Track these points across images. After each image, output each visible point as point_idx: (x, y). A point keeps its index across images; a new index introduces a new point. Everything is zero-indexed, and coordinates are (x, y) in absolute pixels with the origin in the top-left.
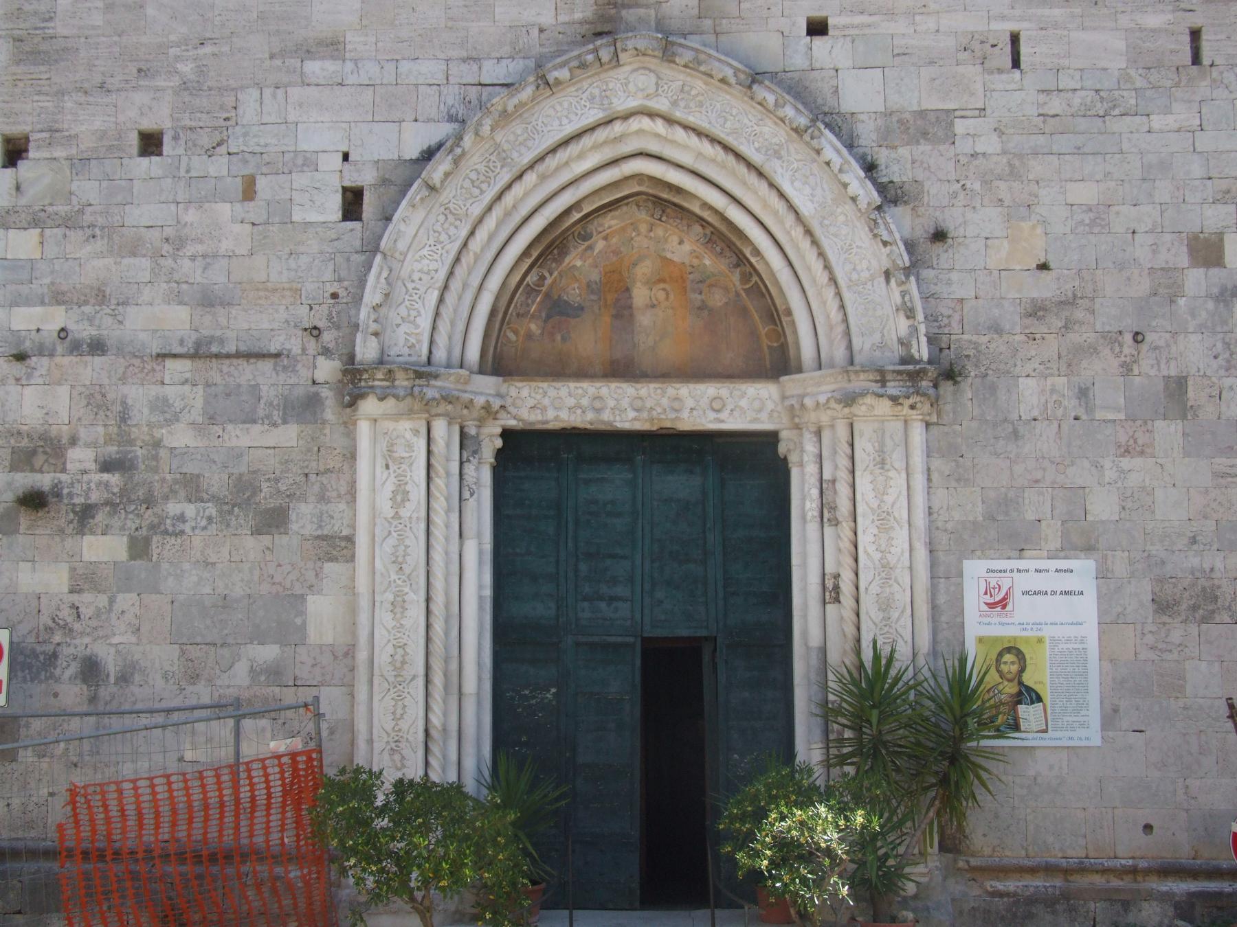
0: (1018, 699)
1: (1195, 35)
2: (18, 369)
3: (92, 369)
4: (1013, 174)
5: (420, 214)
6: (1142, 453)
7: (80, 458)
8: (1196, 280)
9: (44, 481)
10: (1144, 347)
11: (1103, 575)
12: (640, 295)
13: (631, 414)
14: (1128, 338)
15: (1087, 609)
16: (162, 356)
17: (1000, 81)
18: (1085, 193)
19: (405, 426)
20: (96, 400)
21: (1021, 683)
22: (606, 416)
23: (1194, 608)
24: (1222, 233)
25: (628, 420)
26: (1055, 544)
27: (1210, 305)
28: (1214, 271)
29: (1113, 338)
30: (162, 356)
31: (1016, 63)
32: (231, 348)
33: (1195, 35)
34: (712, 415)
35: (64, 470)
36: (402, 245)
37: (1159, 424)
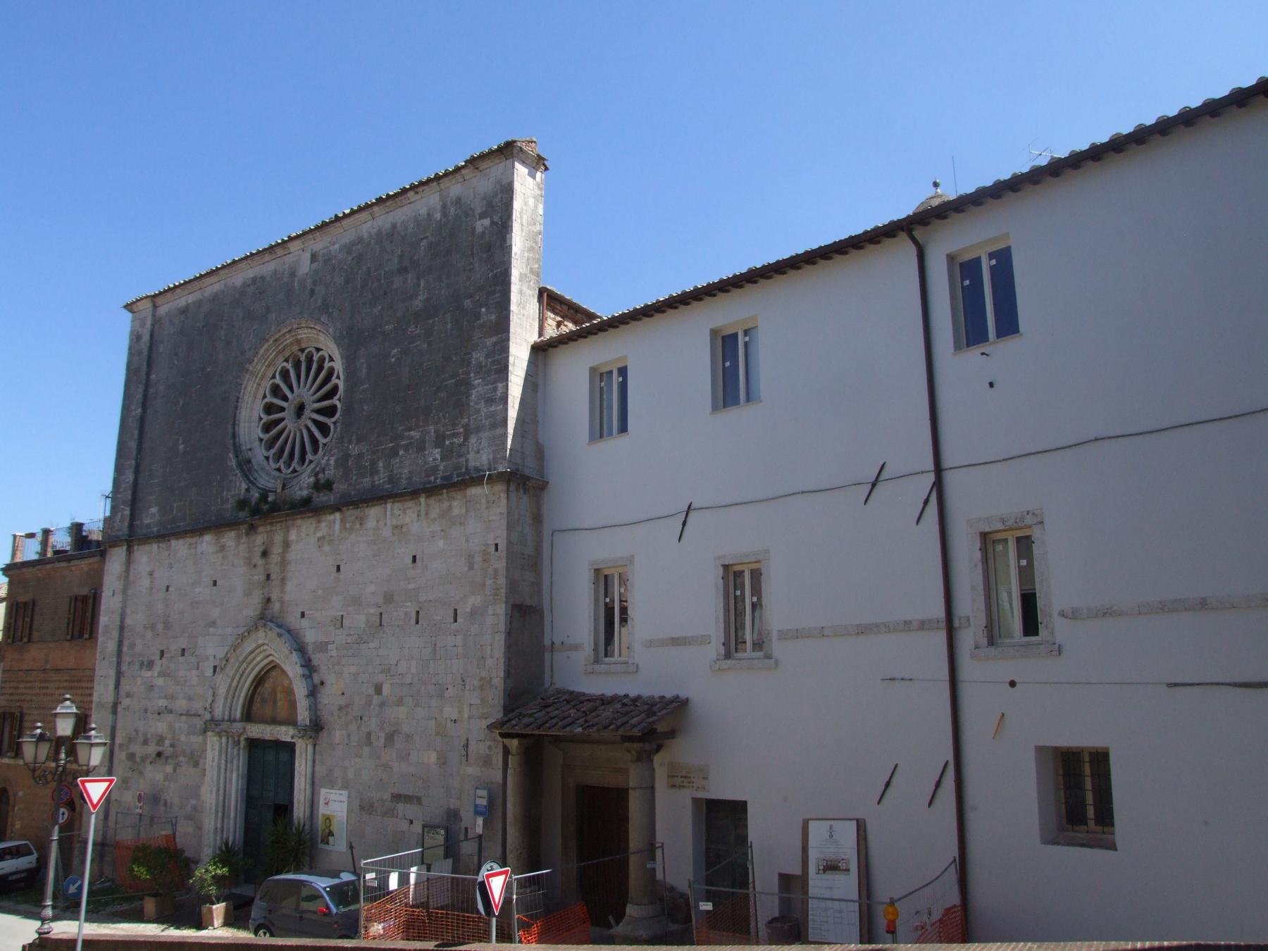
0: (329, 835)
1: (381, 614)
2: (157, 717)
3: (170, 718)
4: (339, 663)
5: (221, 675)
6: (360, 757)
7: (167, 743)
8: (376, 699)
9: (161, 749)
10: (363, 722)
11: (349, 796)
12: (279, 695)
13: (269, 735)
14: (359, 718)
15: (345, 806)
16: (181, 715)
17: (338, 632)
18: (353, 669)
19: (215, 739)
20: (171, 727)
21: (330, 830)
22: (264, 735)
23: (368, 810)
24: (382, 684)
25: (268, 737)
26: (340, 785)
27: (378, 708)
28: (380, 696)
29: (356, 718)
30: (181, 715)
31: (342, 626)
32: (192, 713)
33: (381, 614)
34: (284, 737)
35: (164, 746)
36: (217, 685)
37: (364, 747)
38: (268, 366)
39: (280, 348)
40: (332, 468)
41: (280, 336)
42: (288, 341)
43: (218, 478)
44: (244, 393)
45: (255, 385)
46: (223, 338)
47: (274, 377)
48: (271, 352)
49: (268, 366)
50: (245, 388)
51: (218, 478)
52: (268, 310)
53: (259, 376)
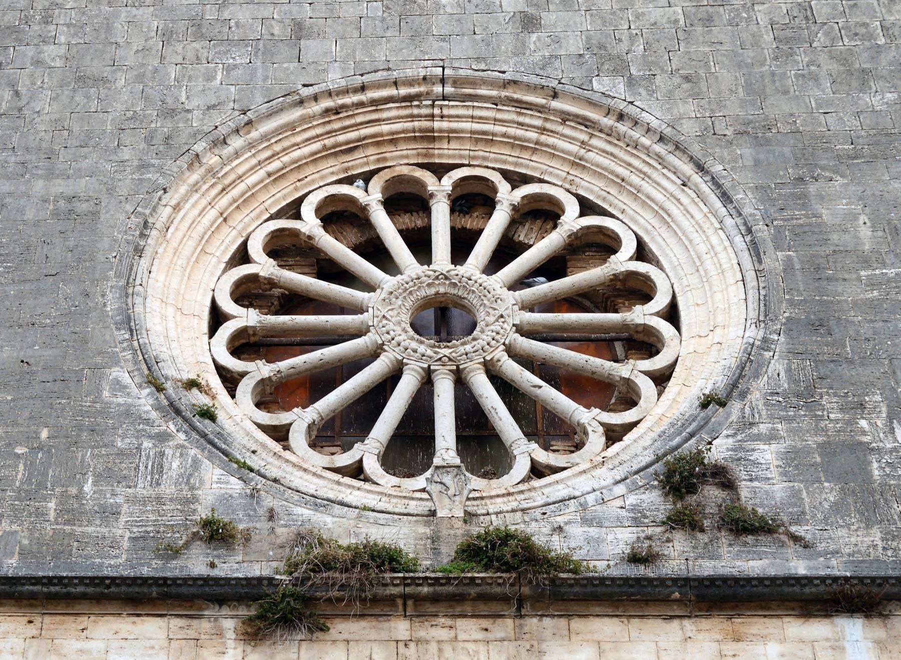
38: (277, 177)
39: (342, 138)
40: (774, 473)
41: (361, 104)
42: (385, 128)
43: (44, 434)
44: (170, 221)
45: (212, 213)
46: (59, 63)
47: (440, 170)
48: (298, 139)
49: (277, 177)
50: (177, 208)
51: (44, 434)
52: (299, 31)
53: (235, 192)
